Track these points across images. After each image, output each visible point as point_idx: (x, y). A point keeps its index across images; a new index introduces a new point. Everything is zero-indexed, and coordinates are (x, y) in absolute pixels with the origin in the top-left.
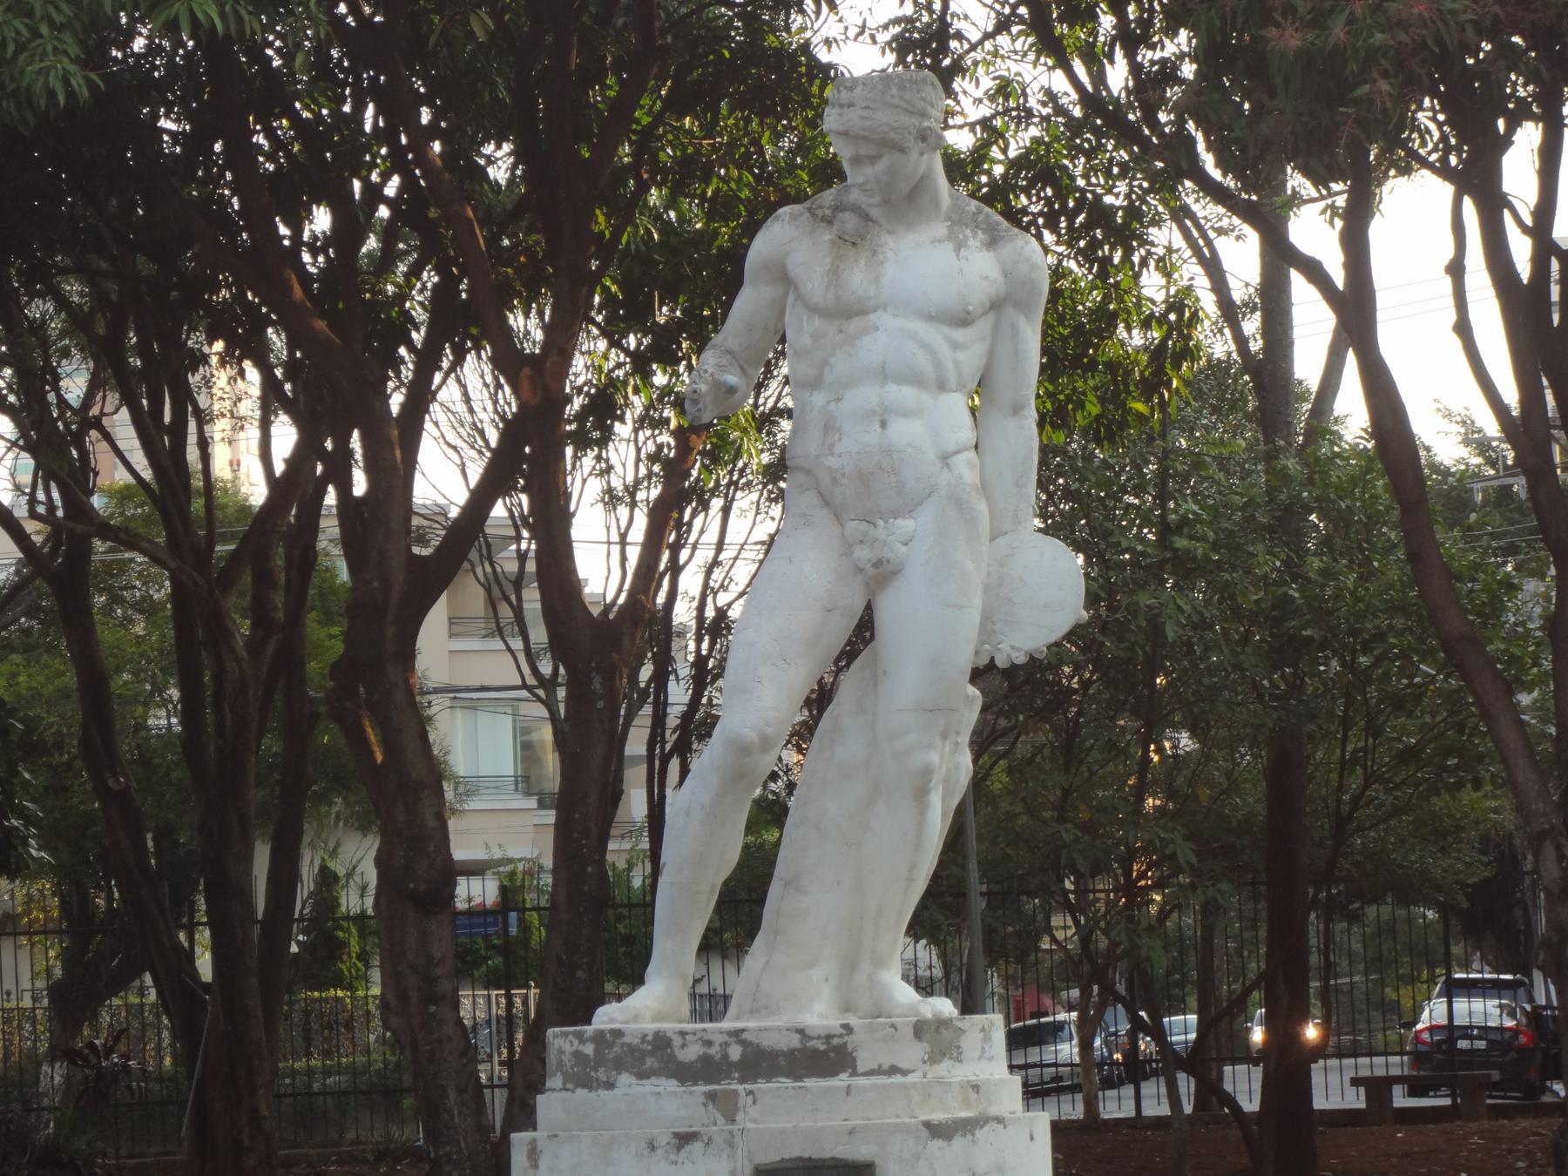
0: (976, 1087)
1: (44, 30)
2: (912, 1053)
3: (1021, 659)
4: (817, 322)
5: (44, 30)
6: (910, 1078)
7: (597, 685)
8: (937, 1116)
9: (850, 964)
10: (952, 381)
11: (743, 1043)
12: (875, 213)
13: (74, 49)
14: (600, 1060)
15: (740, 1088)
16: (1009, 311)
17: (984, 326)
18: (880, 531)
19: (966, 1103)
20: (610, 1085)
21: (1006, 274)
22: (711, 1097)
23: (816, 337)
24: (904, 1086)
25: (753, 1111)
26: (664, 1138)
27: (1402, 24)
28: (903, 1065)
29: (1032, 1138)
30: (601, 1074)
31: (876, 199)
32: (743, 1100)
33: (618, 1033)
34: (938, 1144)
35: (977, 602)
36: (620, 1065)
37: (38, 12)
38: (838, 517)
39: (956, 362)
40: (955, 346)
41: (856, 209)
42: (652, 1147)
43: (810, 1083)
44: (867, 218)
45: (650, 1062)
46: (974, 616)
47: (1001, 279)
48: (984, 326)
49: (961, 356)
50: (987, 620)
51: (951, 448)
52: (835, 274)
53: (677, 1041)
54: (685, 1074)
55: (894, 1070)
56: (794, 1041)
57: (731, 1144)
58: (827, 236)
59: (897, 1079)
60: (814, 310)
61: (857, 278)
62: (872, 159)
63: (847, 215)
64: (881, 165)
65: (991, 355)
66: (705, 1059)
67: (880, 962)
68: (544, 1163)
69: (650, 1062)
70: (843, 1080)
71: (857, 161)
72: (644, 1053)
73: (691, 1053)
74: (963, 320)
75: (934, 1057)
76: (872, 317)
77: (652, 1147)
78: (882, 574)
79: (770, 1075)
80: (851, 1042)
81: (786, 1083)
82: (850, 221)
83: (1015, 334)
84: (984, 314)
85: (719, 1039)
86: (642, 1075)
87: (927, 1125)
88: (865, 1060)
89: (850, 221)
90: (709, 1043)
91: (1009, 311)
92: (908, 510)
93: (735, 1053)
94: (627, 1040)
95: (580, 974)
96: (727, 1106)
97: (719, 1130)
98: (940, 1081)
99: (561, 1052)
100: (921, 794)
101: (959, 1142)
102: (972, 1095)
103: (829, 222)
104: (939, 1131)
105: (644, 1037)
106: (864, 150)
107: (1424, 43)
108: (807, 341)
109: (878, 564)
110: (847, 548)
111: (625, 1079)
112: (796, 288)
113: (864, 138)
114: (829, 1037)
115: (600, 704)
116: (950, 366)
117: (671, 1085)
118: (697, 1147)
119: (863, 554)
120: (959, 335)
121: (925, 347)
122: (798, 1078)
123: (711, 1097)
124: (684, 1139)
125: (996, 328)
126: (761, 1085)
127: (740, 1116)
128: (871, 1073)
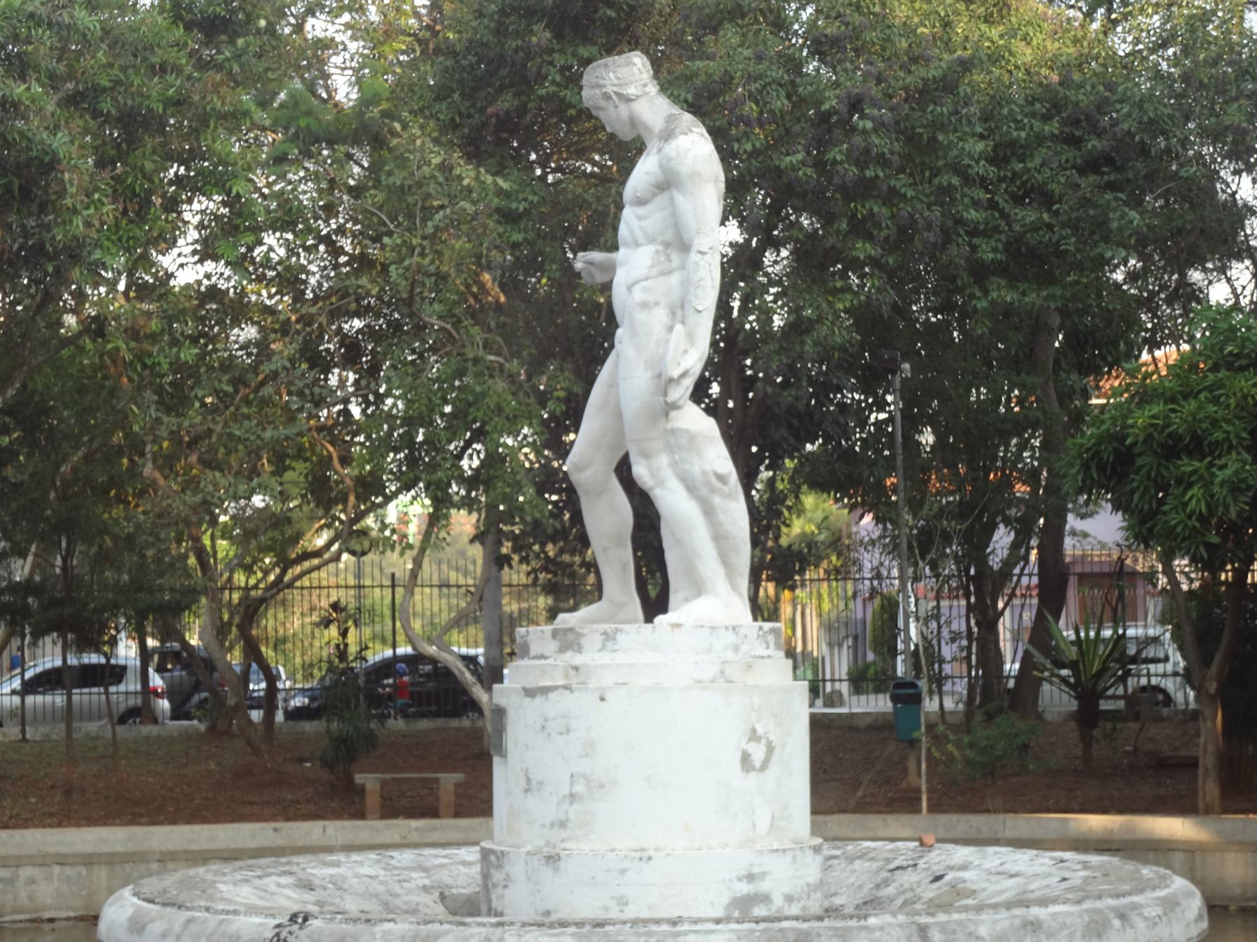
0: (576, 669)
6: (549, 661)
8: (531, 684)
10: (641, 239)
21: (661, 167)
28: (546, 654)
29: (602, 699)
34: (528, 700)
39: (641, 228)
47: (657, 170)
49: (643, 223)
51: (630, 282)
55: (542, 657)
59: (542, 662)
75: (563, 649)
84: (654, 195)
87: (524, 689)
88: (532, 653)
102: (573, 673)
104: (530, 693)
116: (638, 232)
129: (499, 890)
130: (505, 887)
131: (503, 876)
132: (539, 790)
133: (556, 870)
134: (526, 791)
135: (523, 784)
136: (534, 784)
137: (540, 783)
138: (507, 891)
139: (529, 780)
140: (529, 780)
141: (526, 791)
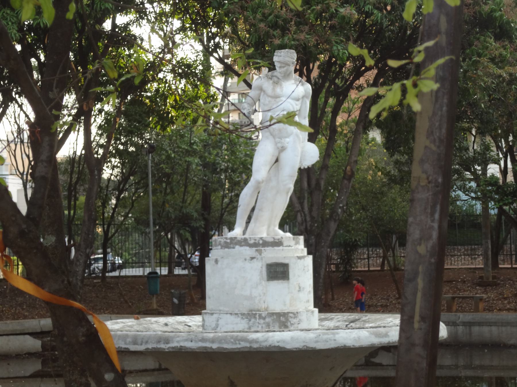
1: (10, 23)
2: (292, 243)
3: (306, 167)
4: (270, 99)
5: (10, 23)
6: (293, 248)
7: (96, 173)
9: (269, 227)
11: (263, 240)
12: (280, 77)
13: (16, 29)
14: (231, 243)
15: (263, 249)
16: (305, 99)
17: (300, 101)
18: (283, 141)
19: (302, 253)
20: (234, 248)
21: (305, 91)
22: (257, 250)
23: (269, 102)
24: (292, 249)
25: (265, 253)
26: (248, 258)
27: (298, 40)
30: (232, 246)
31: (283, 75)
32: (263, 251)
33: (236, 238)
34: (299, 260)
35: (300, 155)
36: (236, 244)
37: (9, 20)
38: (274, 137)
40: (297, 105)
41: (276, 76)
42: (245, 260)
43: (276, 248)
44: (278, 78)
45: (243, 243)
46: (299, 158)
47: (303, 91)
48: (300, 101)
50: (301, 159)
52: (274, 89)
53: (249, 239)
54: (251, 246)
55: (290, 246)
56: (272, 240)
57: (262, 259)
58: (271, 82)
59: (290, 248)
60: (269, 96)
61: (278, 90)
62: (284, 67)
63: (275, 78)
64: (285, 68)
65: (301, 107)
66: (255, 243)
67: (275, 226)
68: (219, 263)
69: (243, 243)
70: (281, 248)
71: (280, 67)
72: (241, 242)
73: (252, 242)
74: (298, 100)
76: (281, 98)
77: (245, 260)
78: (282, 149)
79: (268, 246)
80: (283, 240)
81: (270, 248)
82: (275, 79)
83: (306, 103)
85: (258, 239)
86: (241, 246)
87: (297, 257)
88: (285, 244)
89: (275, 79)
90: (256, 240)
91: (305, 99)
92: (288, 137)
93: (261, 242)
94: (238, 239)
95: (90, 236)
96: (260, 252)
97: (259, 256)
98: (297, 248)
99: (220, 241)
100: (288, 193)
101: (302, 260)
103: (271, 79)
105: (242, 239)
106: (283, 65)
107: (301, 45)
108: (267, 102)
109: (282, 147)
110: (276, 144)
111: (237, 247)
112: (264, 91)
113: (283, 63)
114: (279, 239)
115: (97, 177)
117: (247, 248)
118: (255, 260)
119: (279, 145)
120: (297, 103)
121: (291, 104)
122: (273, 247)
123: (257, 250)
124: (252, 258)
125: (302, 102)
126: (266, 248)
127: (262, 254)
128: (286, 246)
129: (296, 326)
130: (299, 324)
131: (298, 320)
132: (303, 290)
133: (313, 316)
134: (299, 291)
135: (298, 288)
136: (302, 289)
137: (303, 288)
138: (300, 325)
139: (300, 288)
140: (300, 288)
141: (299, 291)
